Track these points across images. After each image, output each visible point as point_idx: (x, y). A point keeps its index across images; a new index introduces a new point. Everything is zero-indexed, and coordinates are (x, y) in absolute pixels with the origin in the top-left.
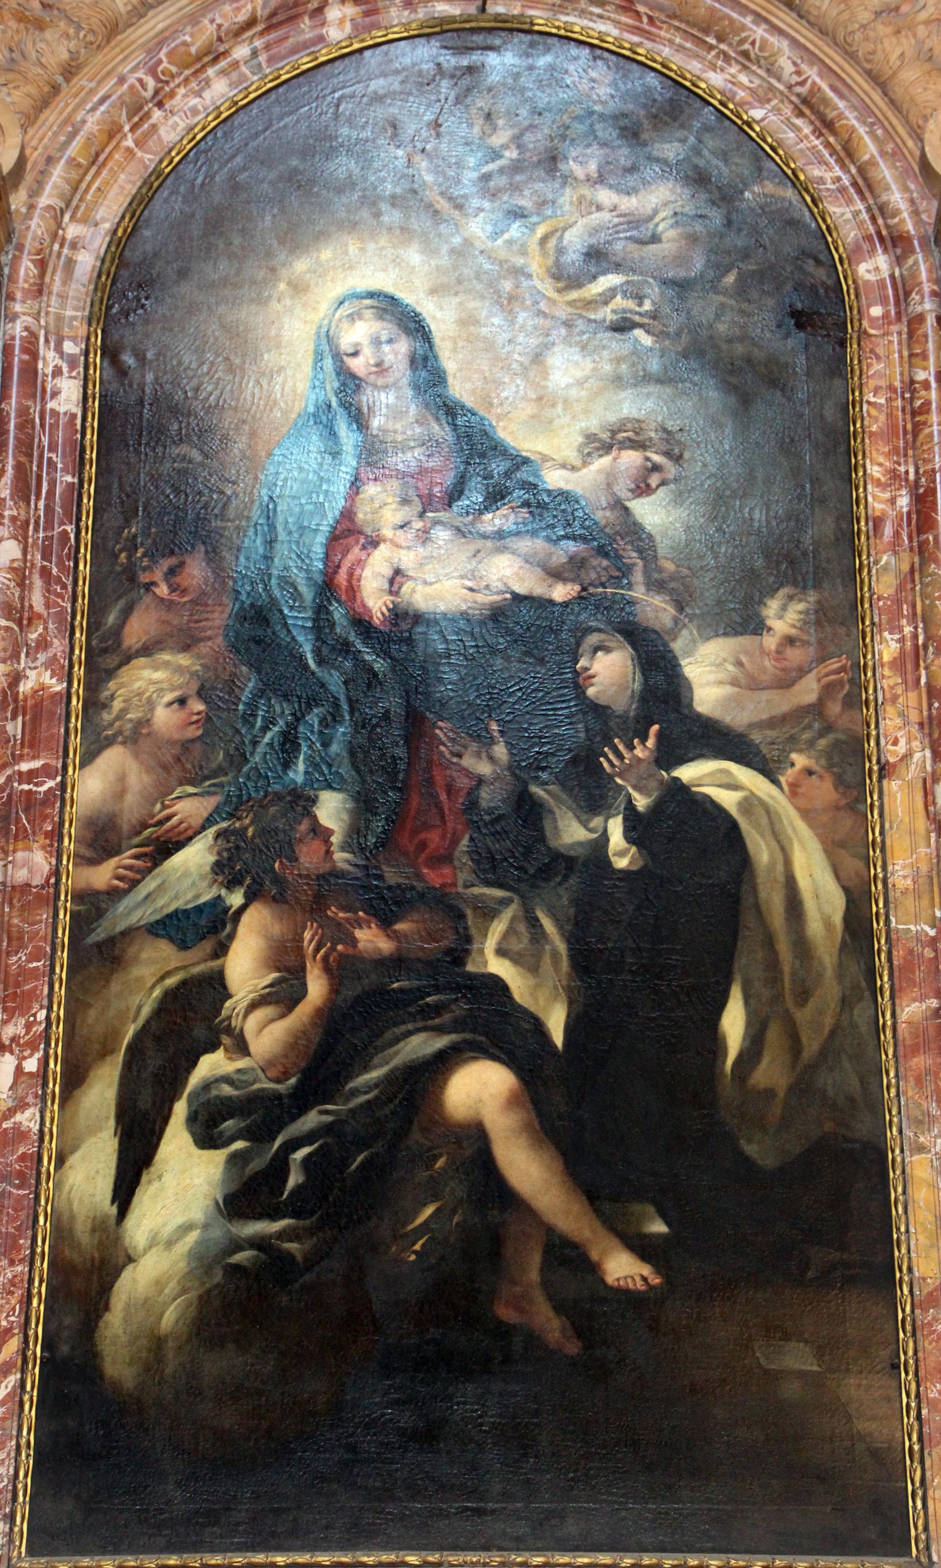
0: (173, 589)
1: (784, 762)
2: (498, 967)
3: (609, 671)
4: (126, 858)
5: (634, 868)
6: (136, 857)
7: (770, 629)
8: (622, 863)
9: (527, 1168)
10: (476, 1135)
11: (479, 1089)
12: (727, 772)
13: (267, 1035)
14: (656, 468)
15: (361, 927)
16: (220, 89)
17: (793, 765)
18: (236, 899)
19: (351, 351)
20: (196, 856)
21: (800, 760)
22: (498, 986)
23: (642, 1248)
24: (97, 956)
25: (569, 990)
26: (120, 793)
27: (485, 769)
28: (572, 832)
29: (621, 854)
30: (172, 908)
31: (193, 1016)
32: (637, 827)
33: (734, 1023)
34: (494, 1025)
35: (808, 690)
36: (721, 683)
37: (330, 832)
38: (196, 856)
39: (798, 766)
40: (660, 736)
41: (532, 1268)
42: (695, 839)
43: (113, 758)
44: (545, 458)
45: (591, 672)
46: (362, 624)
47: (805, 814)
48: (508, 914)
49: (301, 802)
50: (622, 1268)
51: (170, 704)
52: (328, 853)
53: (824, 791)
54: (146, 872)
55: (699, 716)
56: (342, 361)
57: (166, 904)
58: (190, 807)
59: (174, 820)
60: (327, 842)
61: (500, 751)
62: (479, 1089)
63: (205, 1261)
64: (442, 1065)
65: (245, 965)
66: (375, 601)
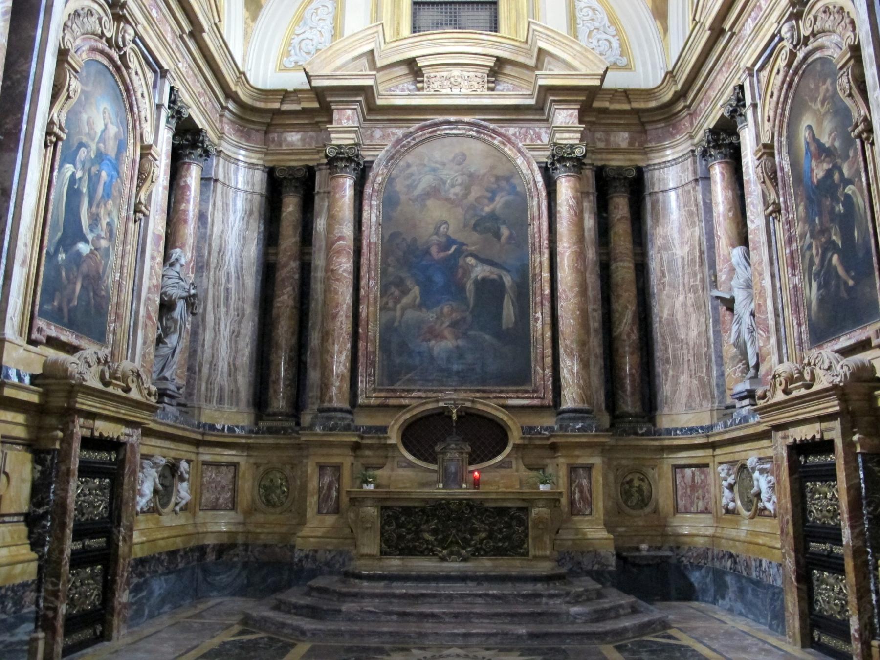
2: (834, 237)
9: (841, 271)
11: (835, 259)
13: (817, 260)
20: (808, 235)
22: (834, 241)
23: (853, 278)
24: (803, 256)
31: (811, 263)
38: (808, 235)
41: (842, 287)
50: (851, 283)
64: (832, 256)
66: (815, 181)
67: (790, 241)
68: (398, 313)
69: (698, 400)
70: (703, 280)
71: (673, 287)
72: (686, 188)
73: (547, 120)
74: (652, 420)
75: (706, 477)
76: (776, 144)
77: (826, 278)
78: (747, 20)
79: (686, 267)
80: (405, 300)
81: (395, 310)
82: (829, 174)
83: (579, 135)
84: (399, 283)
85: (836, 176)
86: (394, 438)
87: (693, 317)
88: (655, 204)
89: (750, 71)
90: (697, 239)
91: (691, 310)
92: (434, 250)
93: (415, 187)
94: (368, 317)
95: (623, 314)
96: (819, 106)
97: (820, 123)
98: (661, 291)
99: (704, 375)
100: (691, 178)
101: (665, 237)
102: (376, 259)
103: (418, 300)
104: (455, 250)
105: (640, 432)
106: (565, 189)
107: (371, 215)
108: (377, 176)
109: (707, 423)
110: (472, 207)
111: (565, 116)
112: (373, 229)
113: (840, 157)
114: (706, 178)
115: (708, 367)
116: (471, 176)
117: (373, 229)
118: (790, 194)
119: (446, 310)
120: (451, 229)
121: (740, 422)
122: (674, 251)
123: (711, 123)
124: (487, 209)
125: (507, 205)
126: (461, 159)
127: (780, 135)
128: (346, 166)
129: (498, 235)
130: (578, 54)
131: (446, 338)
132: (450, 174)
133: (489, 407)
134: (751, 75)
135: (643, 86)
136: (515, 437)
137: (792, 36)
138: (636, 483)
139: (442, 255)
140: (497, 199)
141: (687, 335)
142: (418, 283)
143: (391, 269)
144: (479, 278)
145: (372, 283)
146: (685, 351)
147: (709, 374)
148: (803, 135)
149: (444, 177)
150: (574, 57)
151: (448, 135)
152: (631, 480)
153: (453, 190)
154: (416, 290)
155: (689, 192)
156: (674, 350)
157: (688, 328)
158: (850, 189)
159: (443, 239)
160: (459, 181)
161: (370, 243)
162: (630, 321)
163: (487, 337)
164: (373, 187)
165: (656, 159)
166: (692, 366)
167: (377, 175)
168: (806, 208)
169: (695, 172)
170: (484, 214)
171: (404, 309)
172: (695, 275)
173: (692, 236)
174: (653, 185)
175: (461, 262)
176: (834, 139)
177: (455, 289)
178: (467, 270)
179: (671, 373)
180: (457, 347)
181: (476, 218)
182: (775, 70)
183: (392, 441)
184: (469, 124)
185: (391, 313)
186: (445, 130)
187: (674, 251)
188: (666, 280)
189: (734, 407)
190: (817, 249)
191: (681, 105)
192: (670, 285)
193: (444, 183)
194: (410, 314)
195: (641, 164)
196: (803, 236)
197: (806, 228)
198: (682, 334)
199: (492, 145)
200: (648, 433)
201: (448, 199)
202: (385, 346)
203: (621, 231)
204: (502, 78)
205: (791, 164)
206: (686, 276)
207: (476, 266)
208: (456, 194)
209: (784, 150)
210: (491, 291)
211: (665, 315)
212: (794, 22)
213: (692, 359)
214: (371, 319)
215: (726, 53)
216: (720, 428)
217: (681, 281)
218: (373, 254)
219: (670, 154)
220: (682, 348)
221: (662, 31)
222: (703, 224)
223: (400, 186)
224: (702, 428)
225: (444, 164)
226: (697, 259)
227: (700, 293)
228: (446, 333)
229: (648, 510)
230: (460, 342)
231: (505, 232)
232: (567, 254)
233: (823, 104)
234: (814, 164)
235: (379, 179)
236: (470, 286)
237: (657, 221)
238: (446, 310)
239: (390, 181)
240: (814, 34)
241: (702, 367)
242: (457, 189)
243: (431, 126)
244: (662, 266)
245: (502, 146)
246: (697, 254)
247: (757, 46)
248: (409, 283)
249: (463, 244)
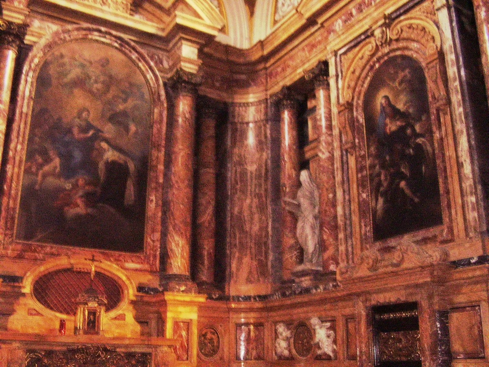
2: (403, 170)
9: (408, 192)
10: (403, 189)
11: (403, 184)
13: (385, 184)
16: (369, 78)
20: (377, 167)
21: (427, 135)
24: (372, 180)
26: (371, 162)
31: (380, 184)
34: (403, 177)
38: (377, 167)
42: (419, 147)
43: (370, 158)
47: (428, 141)
49: (385, 157)
50: (416, 200)
63: (383, 209)
66: (388, 131)
67: (360, 169)
68: (40, 178)
69: (256, 276)
70: (266, 190)
71: (243, 192)
72: (258, 124)
73: (168, 51)
74: (222, 289)
75: (260, 333)
76: (355, 103)
77: (393, 196)
78: (336, 20)
79: (254, 180)
80: (47, 168)
81: (37, 175)
82: (402, 129)
83: (197, 68)
84: (44, 153)
85: (409, 131)
86: (27, 288)
87: (256, 216)
88: (235, 130)
89: (335, 53)
90: (264, 161)
91: (254, 210)
92: (75, 131)
93: (66, 75)
94: (12, 177)
95: (206, 208)
96: (397, 84)
97: (397, 96)
98: (234, 194)
99: (263, 258)
100: (263, 117)
101: (240, 156)
102: (25, 128)
103: (58, 169)
104: (93, 134)
105: (214, 297)
106: (184, 106)
107: (26, 88)
108: (35, 58)
109: (263, 293)
110: (109, 103)
111: (188, 51)
112: (26, 101)
113: (413, 119)
114: (277, 120)
115: (266, 253)
116: (111, 77)
117: (26, 101)
118: (363, 138)
119: (81, 182)
120: (92, 115)
121: (301, 293)
122: (246, 166)
123: (288, 82)
124: (121, 107)
125: (135, 107)
126: (105, 63)
127: (358, 99)
128: (13, 41)
129: (127, 129)
130: (206, 10)
131: (78, 206)
132: (94, 72)
133: (111, 267)
134: (336, 55)
135: (238, 46)
136: (131, 293)
137: (382, 37)
138: (209, 336)
139: (82, 136)
140: (130, 101)
141: (251, 228)
142: (60, 155)
143: (37, 139)
144: (109, 160)
145: (19, 147)
146: (249, 240)
147: (266, 257)
148: (380, 100)
149: (91, 74)
150: (203, 11)
151: (97, 41)
152: (206, 333)
153: (95, 86)
154: (57, 161)
155: (260, 127)
156: (240, 238)
157: (252, 223)
158: (421, 141)
159: (83, 124)
160: (102, 79)
161: (21, 113)
162: (211, 213)
163: (112, 210)
164: (30, 66)
165: (239, 99)
166: (253, 251)
167: (35, 56)
168: (377, 149)
169: (266, 114)
170: (118, 110)
171: (44, 176)
172: (260, 186)
173: (260, 158)
174: (234, 116)
175: (96, 145)
176: (409, 107)
177: (89, 164)
178: (101, 152)
179: (237, 255)
180: (87, 214)
181: (111, 112)
182: (360, 55)
183: (24, 291)
184: (116, 37)
185: (34, 177)
186: (95, 36)
187: (246, 166)
188: (238, 187)
189: (293, 281)
190: (386, 176)
191: (261, 66)
192: (240, 191)
193: (90, 78)
194: (52, 181)
195: (227, 100)
196: (372, 167)
197: (376, 162)
198: (247, 227)
199: (130, 58)
200: (220, 299)
201: (90, 92)
202: (24, 204)
203: (209, 146)
204: (141, 10)
205: (365, 118)
206: (253, 186)
207: (108, 151)
208: (98, 90)
209: (360, 110)
210: (116, 171)
211: (236, 210)
212: (384, 29)
213: (253, 246)
214: (15, 178)
215: (311, 39)
216: (277, 296)
217: (249, 188)
218: (23, 121)
219: (252, 98)
220: (246, 237)
221: (249, 14)
222: (269, 152)
223: (52, 71)
224: (259, 296)
225: (91, 63)
226: (263, 174)
227: (264, 199)
228: (79, 201)
229: (217, 357)
230: (90, 210)
231: (133, 128)
232: (182, 154)
233: (400, 84)
234: (388, 121)
235: (36, 61)
236: (101, 165)
237: (235, 144)
238: (81, 182)
239: (45, 65)
240: (397, 40)
241: (261, 252)
242: (99, 86)
243: (85, 29)
244: (236, 175)
245: (137, 61)
246: (263, 171)
247: (346, 38)
248: (51, 153)
249: (98, 131)
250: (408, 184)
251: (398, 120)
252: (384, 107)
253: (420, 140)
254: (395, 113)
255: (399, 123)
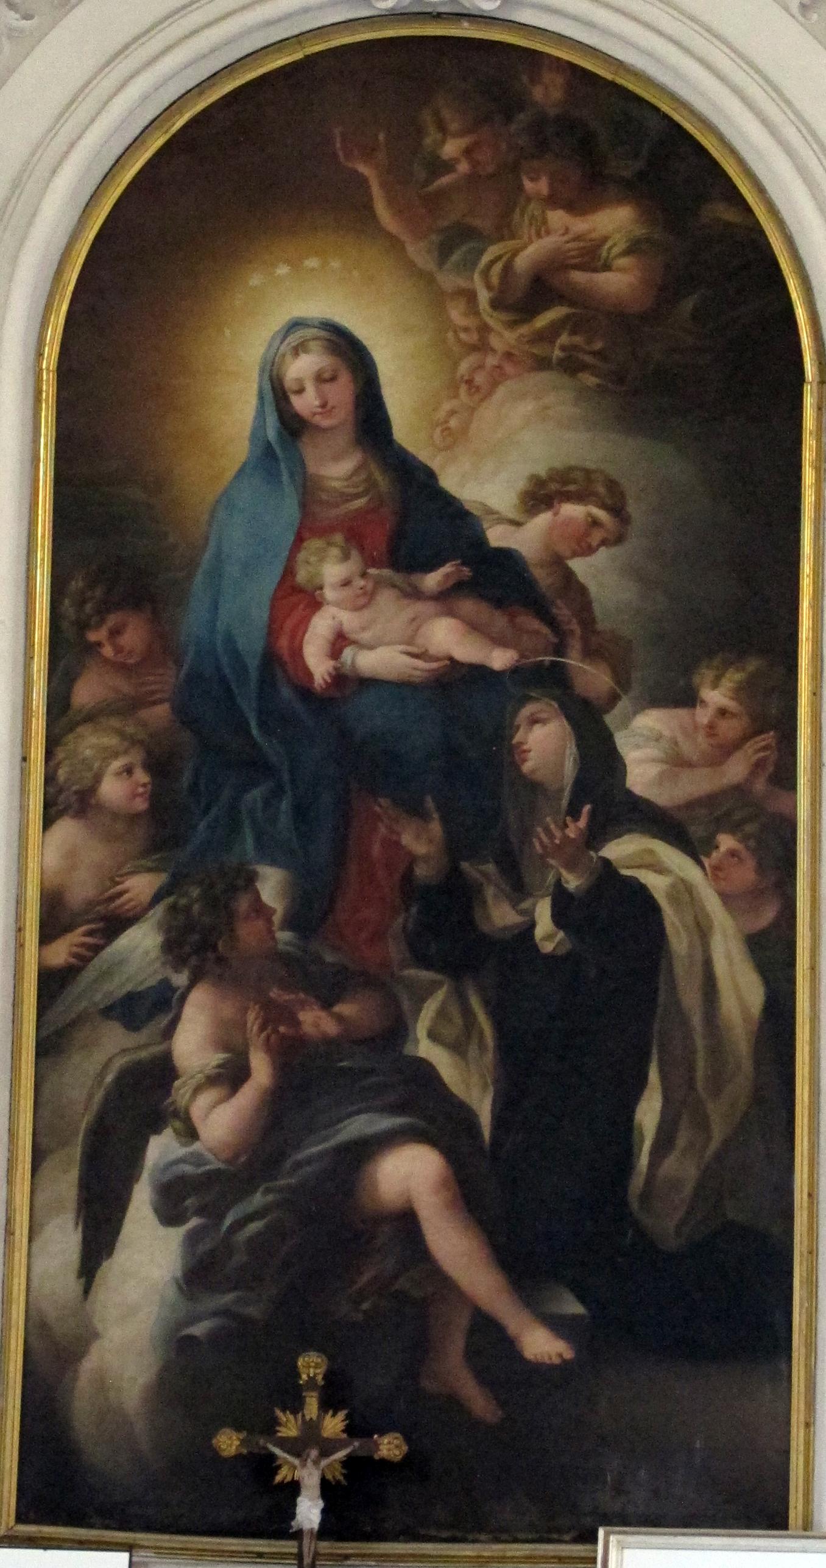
0: (118, 650)
1: (711, 844)
3: (544, 742)
4: (76, 937)
5: (559, 953)
6: (90, 933)
7: (703, 702)
8: (548, 947)
10: (406, 1220)
11: (409, 1173)
12: (651, 852)
14: (595, 523)
15: (303, 1009)
17: (717, 847)
18: (180, 979)
19: (295, 387)
21: (726, 842)
25: (496, 1082)
27: (420, 848)
28: (501, 915)
29: (549, 937)
30: (124, 991)
31: (145, 1096)
32: (565, 907)
33: (648, 1113)
35: (736, 770)
36: (653, 760)
37: (273, 911)
39: (723, 848)
40: (593, 814)
44: (490, 512)
45: (525, 747)
46: (305, 692)
48: (440, 995)
51: (118, 774)
52: (270, 932)
53: (745, 874)
54: (97, 949)
55: (629, 793)
56: (286, 399)
57: (117, 987)
58: (141, 885)
59: (126, 896)
60: (269, 921)
61: (436, 828)
62: (409, 1173)
65: (193, 1043)
66: (318, 664)
197: (141, 885)
250: (468, 1191)
251: (445, 598)
252: (294, 427)
253: (657, 866)
254: (418, 529)
255: (448, 638)
